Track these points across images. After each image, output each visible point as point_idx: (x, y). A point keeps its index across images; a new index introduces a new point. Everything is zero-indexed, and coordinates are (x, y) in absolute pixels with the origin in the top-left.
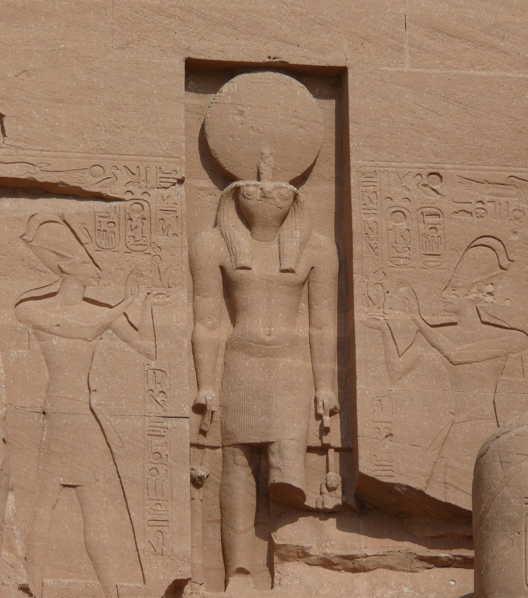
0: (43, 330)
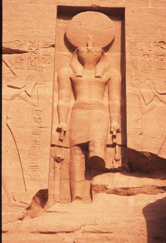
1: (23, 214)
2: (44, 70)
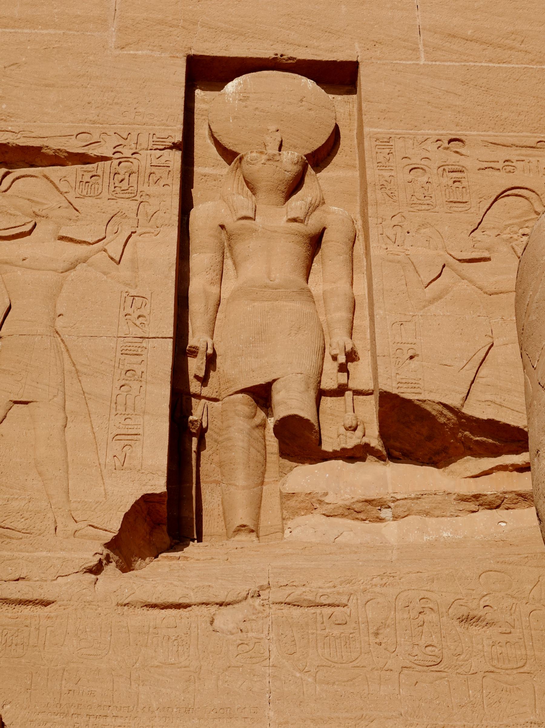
1: (98, 557)
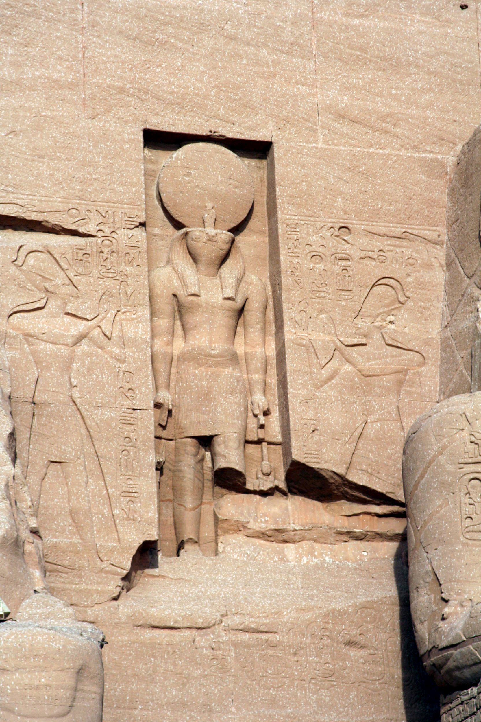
0: (32, 336)
1: (119, 589)
2: (130, 280)
